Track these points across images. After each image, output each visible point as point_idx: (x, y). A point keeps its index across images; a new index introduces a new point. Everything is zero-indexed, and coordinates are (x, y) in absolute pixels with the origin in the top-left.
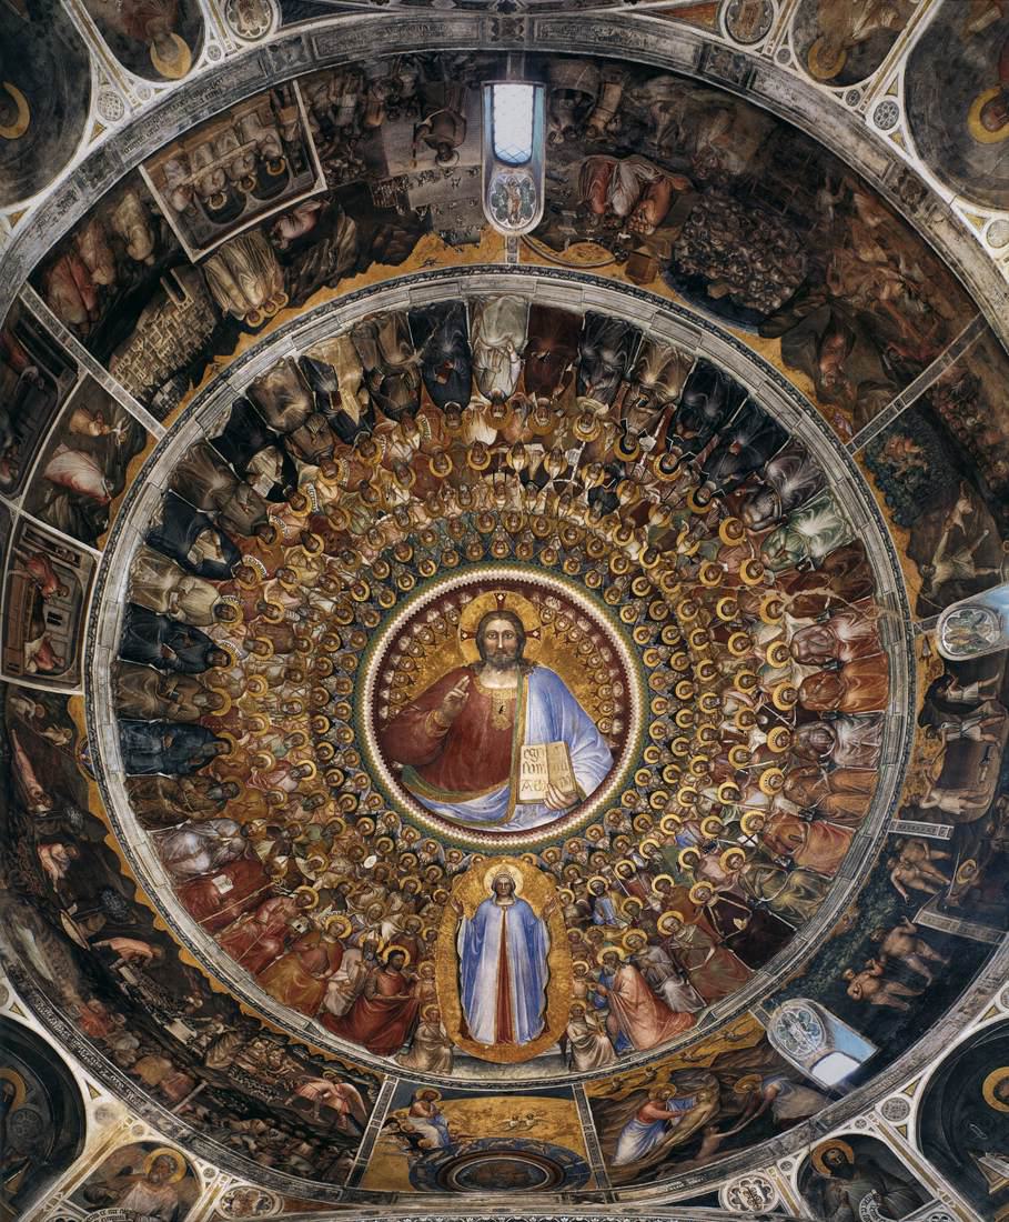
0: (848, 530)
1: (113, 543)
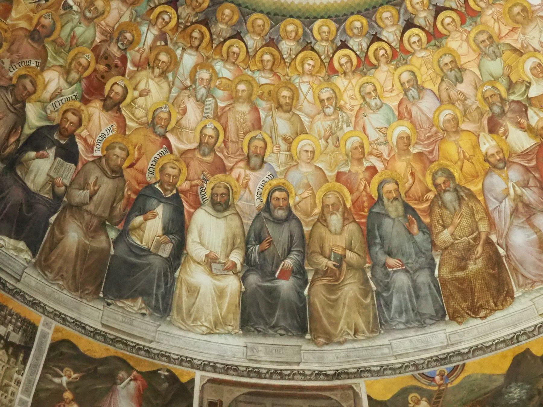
1: (181, 361)
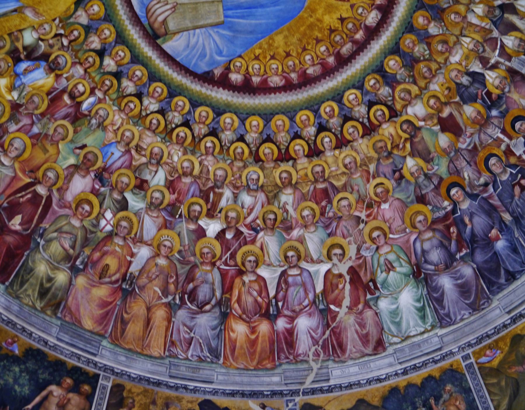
0: (395, 340)
